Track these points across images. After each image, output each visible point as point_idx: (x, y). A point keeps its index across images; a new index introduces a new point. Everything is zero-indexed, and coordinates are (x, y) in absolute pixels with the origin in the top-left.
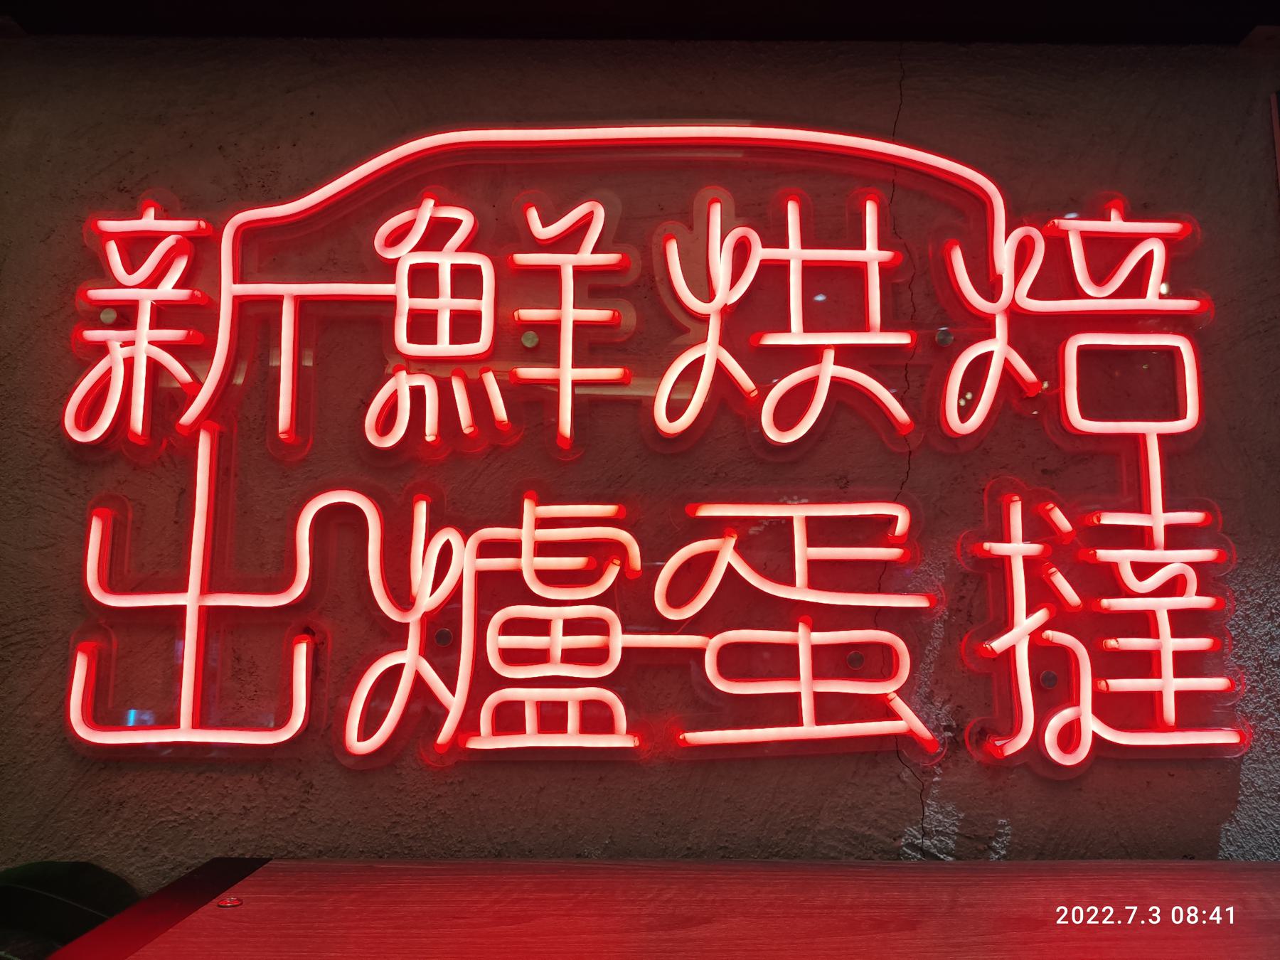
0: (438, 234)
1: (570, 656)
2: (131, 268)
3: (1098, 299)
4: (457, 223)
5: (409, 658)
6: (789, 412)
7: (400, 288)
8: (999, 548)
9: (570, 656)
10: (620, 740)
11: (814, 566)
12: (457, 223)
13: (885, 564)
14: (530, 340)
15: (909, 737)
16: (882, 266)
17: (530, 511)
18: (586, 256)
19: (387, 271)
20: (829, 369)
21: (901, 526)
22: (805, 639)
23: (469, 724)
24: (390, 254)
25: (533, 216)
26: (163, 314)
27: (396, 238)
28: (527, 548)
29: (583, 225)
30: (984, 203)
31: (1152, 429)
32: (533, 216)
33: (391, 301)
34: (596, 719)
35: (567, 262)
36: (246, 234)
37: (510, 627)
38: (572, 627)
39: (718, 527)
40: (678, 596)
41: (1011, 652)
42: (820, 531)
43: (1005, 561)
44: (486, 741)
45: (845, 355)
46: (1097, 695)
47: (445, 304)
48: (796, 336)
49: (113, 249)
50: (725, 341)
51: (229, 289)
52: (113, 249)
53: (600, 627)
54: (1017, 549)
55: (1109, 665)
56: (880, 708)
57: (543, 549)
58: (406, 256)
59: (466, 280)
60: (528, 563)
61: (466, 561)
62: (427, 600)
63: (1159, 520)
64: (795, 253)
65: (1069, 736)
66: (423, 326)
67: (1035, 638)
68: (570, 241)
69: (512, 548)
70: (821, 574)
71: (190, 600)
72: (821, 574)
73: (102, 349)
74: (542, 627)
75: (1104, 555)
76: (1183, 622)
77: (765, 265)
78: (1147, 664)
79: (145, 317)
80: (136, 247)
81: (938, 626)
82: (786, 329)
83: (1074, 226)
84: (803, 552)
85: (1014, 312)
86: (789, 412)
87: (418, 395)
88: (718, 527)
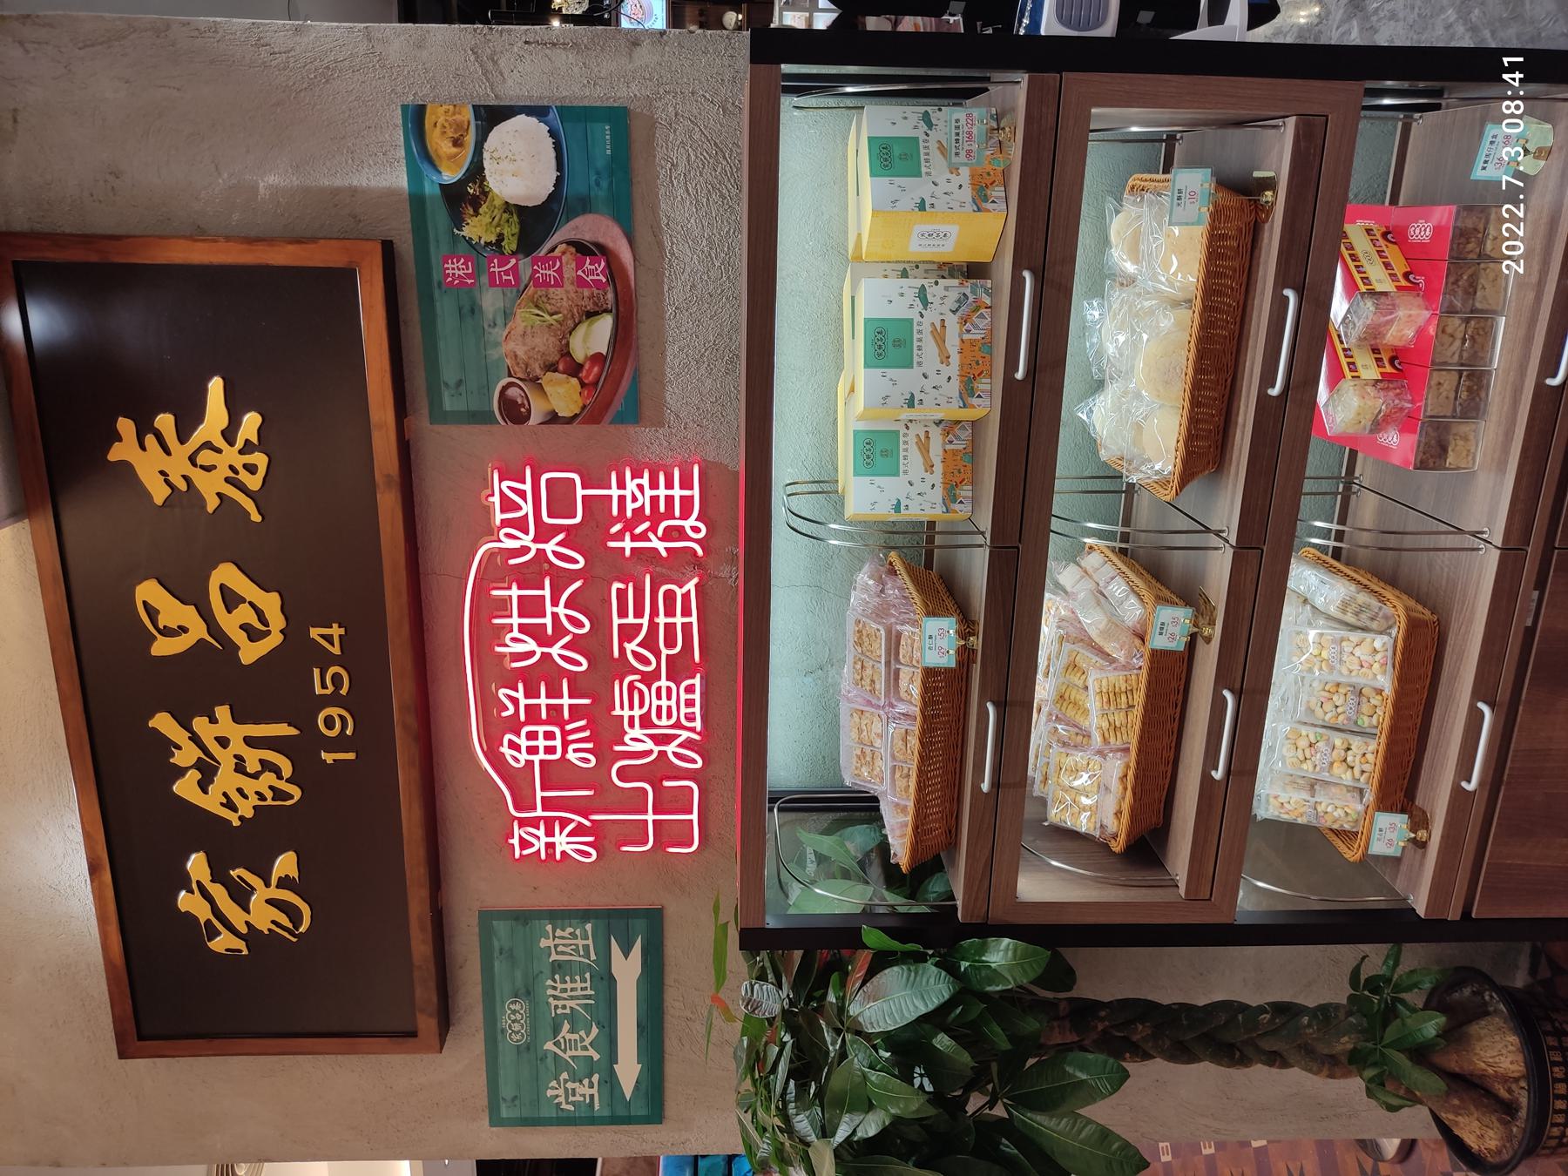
0: (514, 746)
1: (669, 698)
2: (532, 845)
3: (528, 508)
4: (510, 741)
5: (670, 749)
6: (577, 623)
7: (536, 759)
8: (628, 553)
9: (669, 698)
10: (697, 681)
11: (636, 616)
12: (510, 741)
13: (635, 588)
14: (553, 713)
15: (697, 586)
16: (519, 588)
17: (617, 712)
18: (520, 695)
19: (530, 763)
20: (561, 610)
21: (621, 586)
22: (662, 620)
23: (692, 730)
24: (523, 763)
25: (504, 714)
26: (550, 833)
27: (517, 760)
28: (631, 713)
29: (509, 697)
30: (491, 554)
31: (580, 492)
32: (504, 714)
33: (542, 762)
34: (690, 689)
35: (523, 702)
36: (517, 808)
37: (659, 716)
38: (659, 697)
39: (622, 650)
40: (648, 662)
41: (667, 549)
42: (623, 613)
43: (633, 549)
44: (698, 724)
45: (555, 603)
46: (681, 518)
47: (541, 743)
48: (548, 620)
49: (525, 852)
50: (551, 645)
51: (539, 812)
52: (525, 852)
53: (659, 689)
54: (627, 544)
56: (686, 596)
57: (631, 707)
58: (523, 757)
59: (532, 736)
60: (637, 712)
61: (637, 732)
62: (649, 745)
63: (615, 492)
65: (696, 530)
67: (661, 539)
68: (515, 701)
69: (631, 718)
70: (639, 613)
72: (639, 613)
73: (563, 853)
74: (659, 708)
75: (629, 514)
76: (654, 485)
77: (520, 631)
78: (669, 499)
79: (550, 840)
80: (524, 844)
81: (658, 569)
82: (545, 625)
83: (499, 517)
84: (631, 620)
85: (535, 541)
86: (577, 623)
87: (575, 751)
88: (622, 650)
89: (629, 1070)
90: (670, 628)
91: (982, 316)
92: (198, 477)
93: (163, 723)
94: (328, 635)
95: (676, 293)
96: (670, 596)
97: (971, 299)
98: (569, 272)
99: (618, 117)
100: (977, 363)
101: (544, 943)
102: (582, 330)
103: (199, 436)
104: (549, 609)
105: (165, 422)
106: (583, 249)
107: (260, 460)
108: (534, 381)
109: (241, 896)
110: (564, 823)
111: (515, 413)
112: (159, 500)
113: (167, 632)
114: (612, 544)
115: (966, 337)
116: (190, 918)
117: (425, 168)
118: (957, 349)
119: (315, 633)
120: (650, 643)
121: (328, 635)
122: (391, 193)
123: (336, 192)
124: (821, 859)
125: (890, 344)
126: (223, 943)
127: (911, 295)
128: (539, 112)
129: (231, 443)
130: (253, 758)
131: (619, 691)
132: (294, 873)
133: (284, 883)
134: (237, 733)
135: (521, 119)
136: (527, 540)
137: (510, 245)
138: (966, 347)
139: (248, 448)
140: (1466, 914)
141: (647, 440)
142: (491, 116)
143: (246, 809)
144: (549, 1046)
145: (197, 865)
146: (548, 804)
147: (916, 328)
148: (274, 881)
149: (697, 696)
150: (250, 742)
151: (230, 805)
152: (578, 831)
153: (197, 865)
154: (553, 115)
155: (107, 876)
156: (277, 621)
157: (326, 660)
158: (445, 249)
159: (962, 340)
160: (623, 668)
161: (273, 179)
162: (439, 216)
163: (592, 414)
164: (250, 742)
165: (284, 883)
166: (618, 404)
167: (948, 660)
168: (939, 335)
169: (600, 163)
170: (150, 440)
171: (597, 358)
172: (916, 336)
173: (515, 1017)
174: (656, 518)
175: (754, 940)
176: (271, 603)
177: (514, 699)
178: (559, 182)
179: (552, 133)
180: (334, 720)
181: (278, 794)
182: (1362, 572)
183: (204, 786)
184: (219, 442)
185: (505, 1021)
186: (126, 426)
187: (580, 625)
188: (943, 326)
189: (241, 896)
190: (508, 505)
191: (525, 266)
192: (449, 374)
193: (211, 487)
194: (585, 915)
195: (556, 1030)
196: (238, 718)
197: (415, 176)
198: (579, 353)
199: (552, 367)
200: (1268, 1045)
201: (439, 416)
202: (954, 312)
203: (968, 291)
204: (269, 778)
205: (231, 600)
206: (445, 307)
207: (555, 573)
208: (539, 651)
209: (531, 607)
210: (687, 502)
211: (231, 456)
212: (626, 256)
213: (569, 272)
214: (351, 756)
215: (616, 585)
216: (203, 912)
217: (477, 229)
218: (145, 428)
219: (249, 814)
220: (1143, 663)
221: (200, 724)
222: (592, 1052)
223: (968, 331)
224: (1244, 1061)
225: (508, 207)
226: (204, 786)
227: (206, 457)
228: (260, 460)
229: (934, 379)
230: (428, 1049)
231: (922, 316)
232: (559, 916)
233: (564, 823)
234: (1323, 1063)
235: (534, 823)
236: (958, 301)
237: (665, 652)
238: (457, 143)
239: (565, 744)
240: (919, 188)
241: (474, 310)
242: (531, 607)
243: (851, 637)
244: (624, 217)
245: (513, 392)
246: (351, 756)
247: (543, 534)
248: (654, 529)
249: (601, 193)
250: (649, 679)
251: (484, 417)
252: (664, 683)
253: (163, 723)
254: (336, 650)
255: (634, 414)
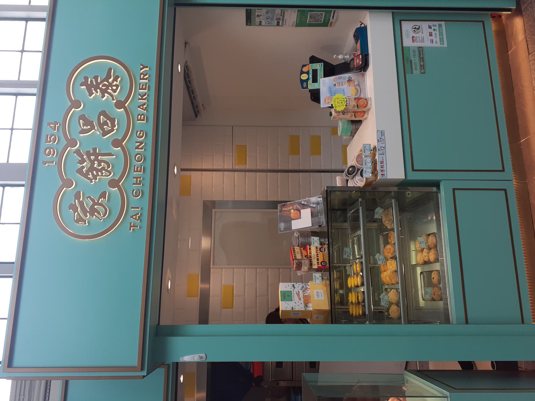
91: (308, 290)
97: (305, 287)
100: (308, 300)
115: (304, 294)
118: (302, 297)
125: (287, 296)
147: (292, 293)
159: (304, 295)
168: (298, 294)
172: (293, 294)
188: (299, 292)
202: (301, 289)
203: (304, 285)
223: (305, 293)
229: (297, 304)
231: (294, 290)
236: (302, 287)
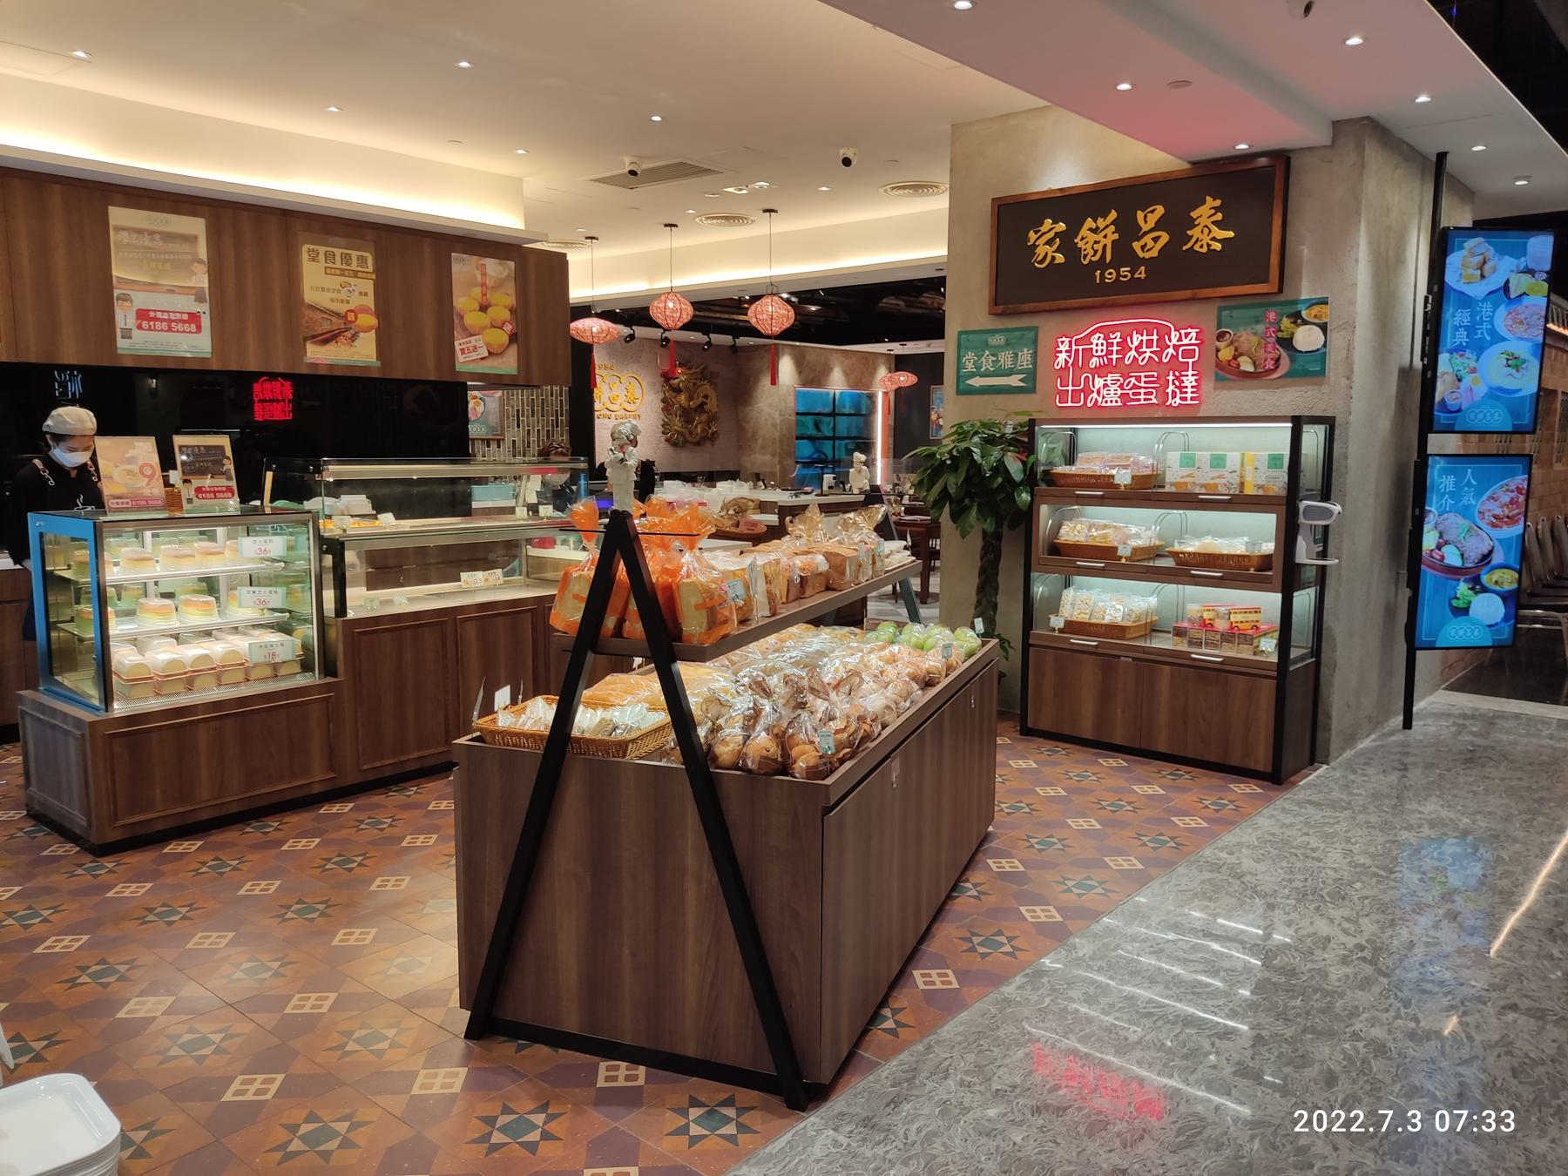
3: (1186, 341)
5: (1095, 395)
10: (1119, 404)
18: (1118, 340)
22: (1142, 391)
26: (1066, 351)
31: (1190, 361)
34: (1117, 402)
35: (1115, 341)
42: (1145, 377)
44: (1104, 405)
47: (1099, 348)
48: (1144, 349)
51: (1074, 347)
54: (1171, 378)
55: (1181, 392)
58: (1095, 342)
60: (1109, 383)
62: (1097, 387)
63: (1190, 372)
64: (1145, 338)
66: (1097, 351)
70: (1145, 382)
71: (1070, 388)
72: (1145, 382)
76: (1192, 387)
78: (1186, 393)
80: (1062, 342)
83: (1183, 332)
84: (1143, 379)
85: (1174, 345)
89: (977, 382)
90: (1139, 394)
92: (1199, 228)
93: (1113, 215)
94: (1141, 273)
95: (1260, 393)
96: (1151, 393)
98: (1270, 356)
99: (1322, 373)
101: (1025, 350)
102: (1249, 360)
103: (1214, 228)
104: (1148, 350)
105: (1219, 216)
106: (1277, 360)
107: (1205, 250)
108: (1231, 343)
109: (1050, 242)
110: (1070, 357)
111: (1220, 336)
112: (1192, 214)
113: (1145, 216)
114: (1171, 373)
116: (1041, 224)
117: (1308, 304)
119: (1143, 268)
120: (1135, 387)
121: (1141, 273)
122: (1299, 291)
123: (1301, 273)
124: (1053, 449)
126: (1031, 234)
127: (1234, 468)
128: (1325, 345)
129: (1211, 240)
130: (1099, 247)
131: (1117, 376)
132: (1056, 262)
133: (1053, 258)
134: (1108, 242)
135: (1323, 338)
136: (1174, 341)
137: (1280, 335)
138: (1216, 485)
139: (1209, 245)
140: (1032, 645)
141: (1208, 385)
142: (1324, 328)
143: (1081, 244)
144: (987, 352)
145: (1062, 226)
146: (1077, 351)
148: (1055, 254)
149: (1114, 404)
150: (1105, 246)
151: (1082, 239)
152: (1066, 362)
153: (1062, 226)
154: (1324, 350)
155: (1059, 195)
156: (1147, 255)
157: (1132, 272)
158: (1278, 311)
160: (1125, 376)
161: (1306, 251)
162: (1291, 310)
163: (1219, 364)
164: (1105, 246)
165: (1053, 258)
166: (1221, 373)
167: (1117, 481)
168: (1220, 477)
169: (1307, 367)
170: (1213, 211)
171: (1239, 366)
173: (999, 340)
174: (1180, 388)
175: (1032, 423)
176: (1154, 253)
177: (1116, 338)
178: (1301, 352)
179: (1318, 350)
180: (1111, 275)
181: (1085, 256)
182: (1239, 966)
183: (1090, 230)
184: (1211, 236)
185: (997, 336)
186: (1218, 203)
187: (1143, 360)
189: (1050, 242)
190: (1187, 335)
191: (1272, 340)
192: (1235, 313)
193: (1195, 233)
194: (1035, 365)
195: (992, 355)
196: (1114, 242)
197: (1306, 301)
198: (1241, 359)
199: (1236, 350)
200: (984, 601)
201: (1220, 309)
204: (1092, 252)
205: (1156, 240)
206: (1258, 312)
207: (1162, 351)
208: (1133, 347)
209: (1149, 344)
210: (1185, 399)
211: (1207, 240)
212: (1275, 376)
213: (1270, 356)
214: (1098, 281)
215: (1155, 374)
216: (1044, 229)
217: (1286, 323)
218: (1217, 209)
219: (1079, 246)
220: (1116, 544)
221: (1112, 228)
222: (984, 368)
224: (978, 592)
225: (1293, 334)
226: (1090, 230)
227: (1206, 230)
228: (1205, 250)
230: (990, 310)
232: (1035, 355)
233: (1070, 357)
234: (1046, 473)
235: (1070, 346)
237: (1131, 392)
238: (1315, 316)
239: (1099, 357)
240: (1263, 468)
241: (1258, 322)
242: (1149, 344)
243: (1128, 455)
244: (1289, 375)
245: (1228, 335)
246: (1098, 281)
247: (1176, 347)
248: (1176, 387)
249: (1297, 366)
250: (1121, 387)
251: (1219, 327)
252: (1119, 392)
253: (1113, 215)
254: (1136, 276)
255: (1218, 379)
